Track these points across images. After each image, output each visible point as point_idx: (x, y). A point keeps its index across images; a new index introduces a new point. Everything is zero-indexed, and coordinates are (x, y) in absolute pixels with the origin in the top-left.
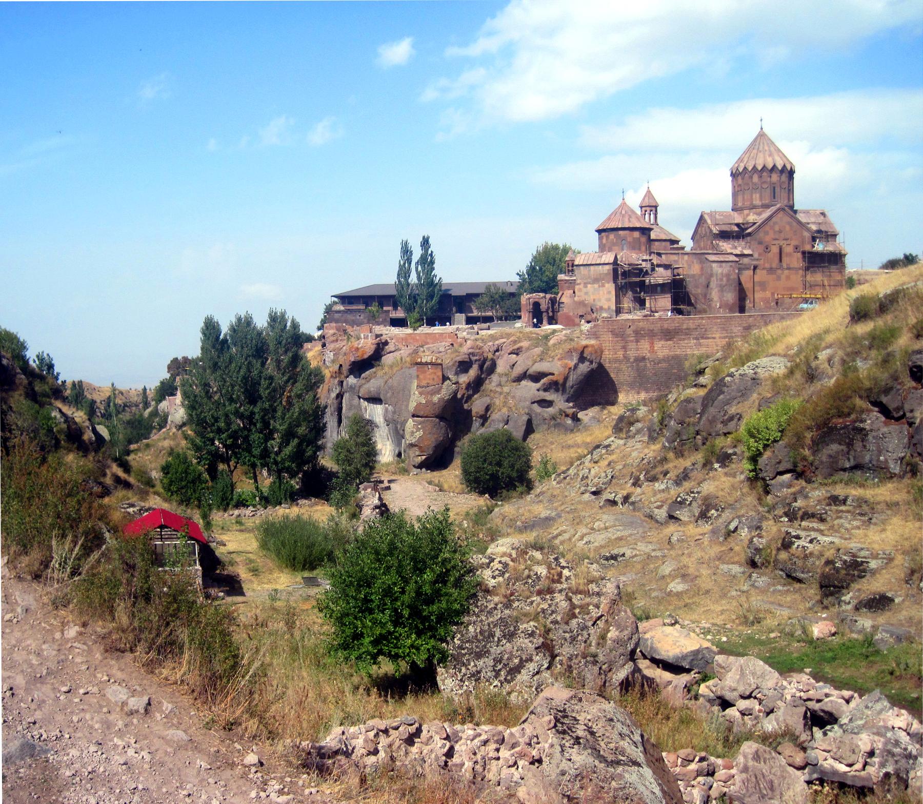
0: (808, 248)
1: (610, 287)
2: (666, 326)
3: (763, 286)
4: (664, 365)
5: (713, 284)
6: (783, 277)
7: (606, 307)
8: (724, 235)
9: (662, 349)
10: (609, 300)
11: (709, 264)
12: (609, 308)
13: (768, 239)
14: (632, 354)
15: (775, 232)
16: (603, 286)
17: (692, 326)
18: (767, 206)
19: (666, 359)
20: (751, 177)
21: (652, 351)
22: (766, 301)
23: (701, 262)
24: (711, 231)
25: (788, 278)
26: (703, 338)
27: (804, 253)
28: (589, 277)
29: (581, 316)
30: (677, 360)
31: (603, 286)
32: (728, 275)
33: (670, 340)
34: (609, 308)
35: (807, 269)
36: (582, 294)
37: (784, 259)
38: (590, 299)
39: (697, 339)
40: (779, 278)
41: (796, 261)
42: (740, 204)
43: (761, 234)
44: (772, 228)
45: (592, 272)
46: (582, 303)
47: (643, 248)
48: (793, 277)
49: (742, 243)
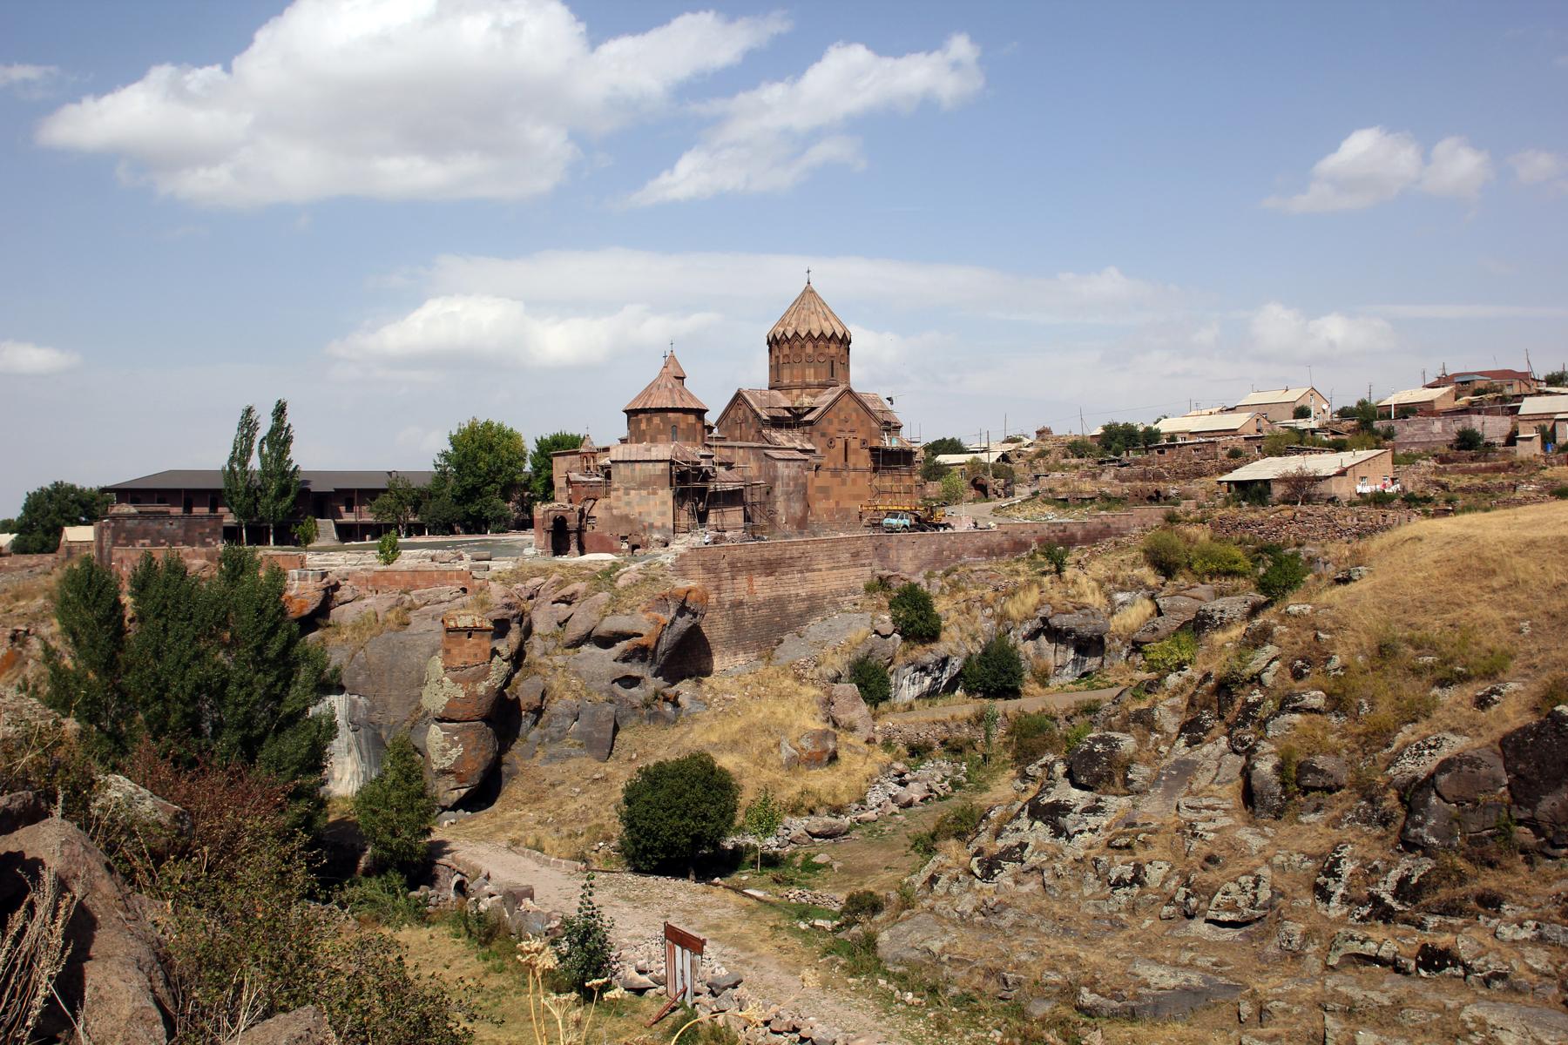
0: (875, 443)
1: (666, 495)
2: (766, 555)
3: (825, 491)
4: (764, 612)
5: (779, 490)
6: (849, 482)
7: (658, 524)
8: (777, 423)
9: (762, 588)
10: (663, 514)
11: (771, 462)
12: (663, 526)
13: (831, 430)
14: (727, 597)
15: (840, 421)
16: (655, 493)
17: (796, 554)
18: (824, 386)
19: (768, 603)
20: (803, 347)
21: (751, 592)
22: (830, 512)
23: (759, 459)
24: (757, 415)
25: (854, 481)
26: (808, 570)
27: (872, 449)
28: (633, 478)
29: (623, 538)
30: (779, 603)
31: (655, 493)
32: (795, 479)
33: (771, 574)
34: (663, 526)
35: (875, 470)
36: (621, 504)
37: (852, 458)
38: (634, 512)
39: (801, 572)
40: (844, 483)
41: (863, 460)
42: (786, 381)
43: (824, 423)
44: (837, 416)
45: (637, 472)
46: (625, 519)
47: (699, 438)
48: (860, 481)
49: (797, 433)
